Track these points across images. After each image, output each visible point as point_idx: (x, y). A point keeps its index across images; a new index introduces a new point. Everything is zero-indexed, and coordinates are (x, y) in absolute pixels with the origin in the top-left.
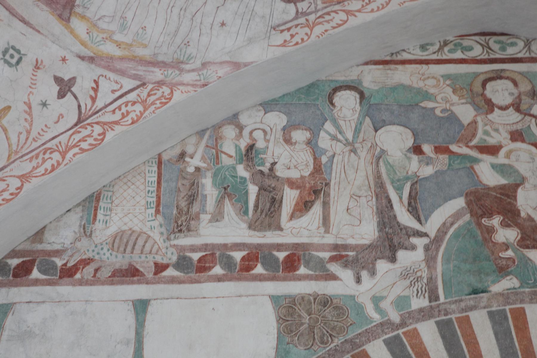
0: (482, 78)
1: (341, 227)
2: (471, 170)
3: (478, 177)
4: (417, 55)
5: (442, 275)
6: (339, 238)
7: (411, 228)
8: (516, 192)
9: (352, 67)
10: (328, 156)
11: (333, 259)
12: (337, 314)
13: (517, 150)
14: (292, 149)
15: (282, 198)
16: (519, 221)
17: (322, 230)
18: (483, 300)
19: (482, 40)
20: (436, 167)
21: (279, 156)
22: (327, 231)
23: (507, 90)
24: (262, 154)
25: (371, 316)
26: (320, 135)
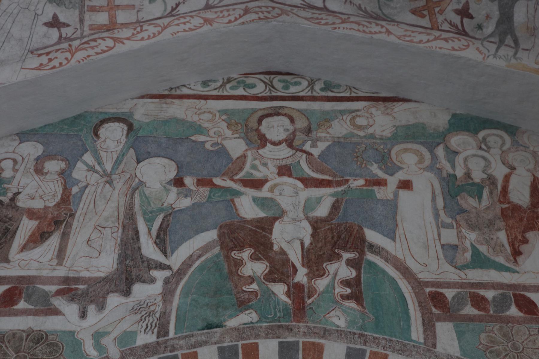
0: (260, 113)
1: (77, 259)
2: (231, 203)
3: (236, 210)
4: (197, 90)
5: (177, 309)
6: (71, 270)
7: (154, 260)
8: (272, 224)
9: (125, 100)
10: (80, 187)
11: (59, 293)
12: (50, 352)
13: (283, 185)
14: (41, 179)
15: (17, 229)
16: (270, 255)
17: (55, 262)
18: (215, 336)
19: (267, 79)
20: (195, 199)
21: (26, 185)
22: (60, 264)
23: (283, 126)
24: (6, 184)
25: (88, 353)
26: (77, 166)
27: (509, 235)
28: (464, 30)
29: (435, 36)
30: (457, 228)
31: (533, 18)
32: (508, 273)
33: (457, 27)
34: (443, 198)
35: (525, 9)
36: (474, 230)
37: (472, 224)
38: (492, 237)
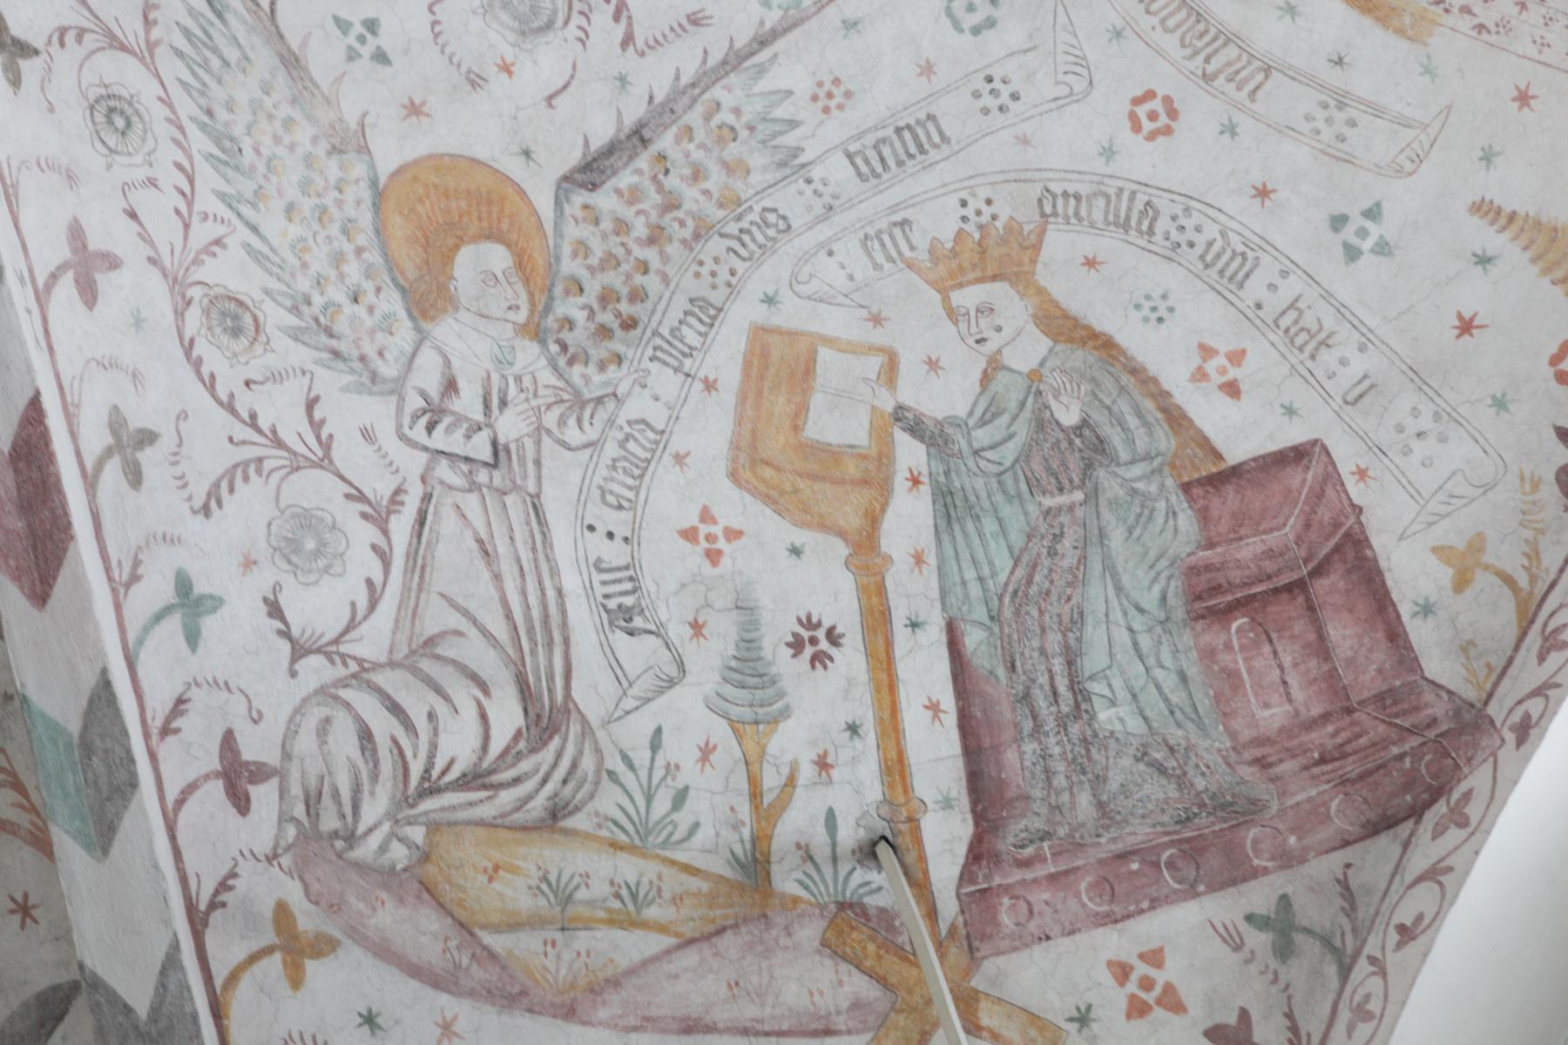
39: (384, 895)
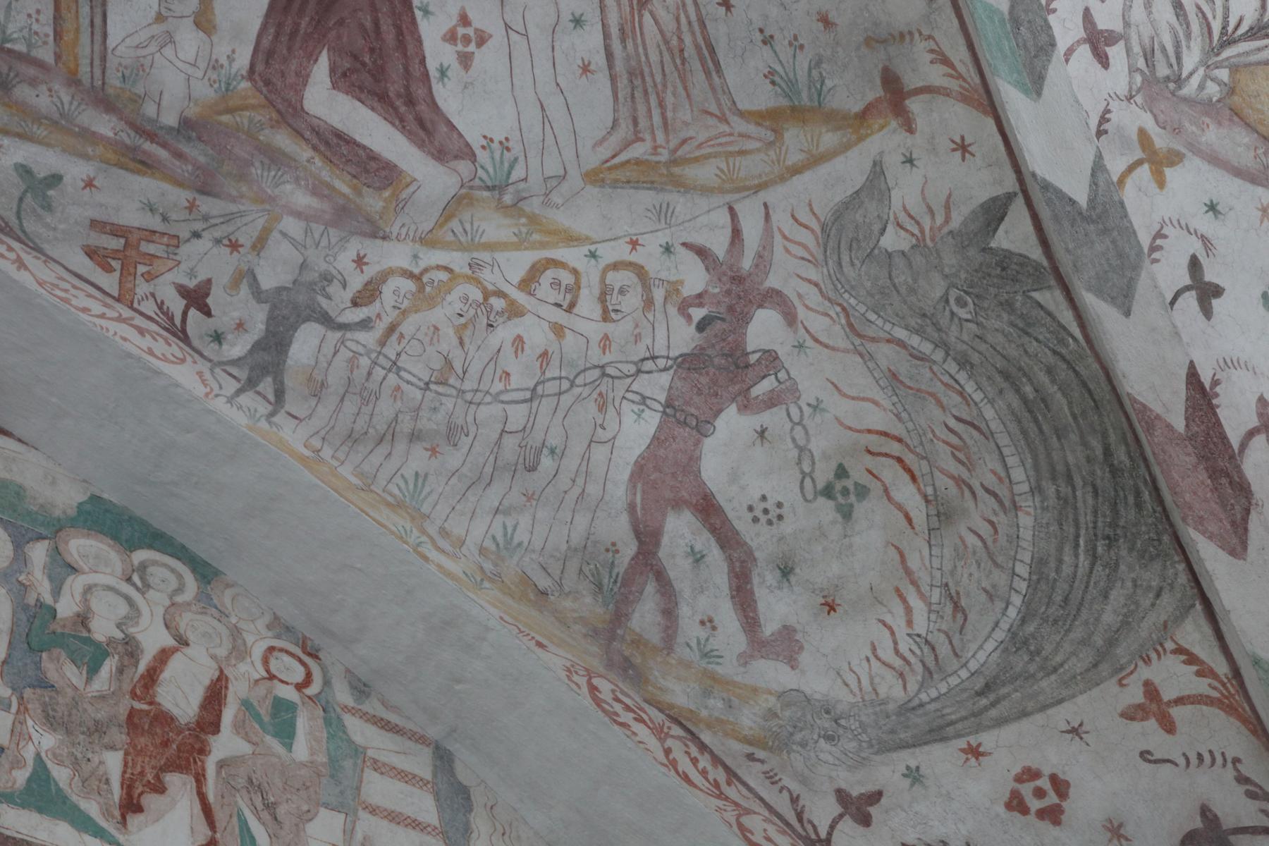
27: (130, 764)
28: (184, 331)
29: (121, 315)
30: (18, 712)
31: (325, 365)
32: (97, 841)
33: (171, 319)
34: (10, 643)
35: (317, 342)
36: (55, 730)
37: (54, 717)
38: (90, 755)
39: (1207, 120)
